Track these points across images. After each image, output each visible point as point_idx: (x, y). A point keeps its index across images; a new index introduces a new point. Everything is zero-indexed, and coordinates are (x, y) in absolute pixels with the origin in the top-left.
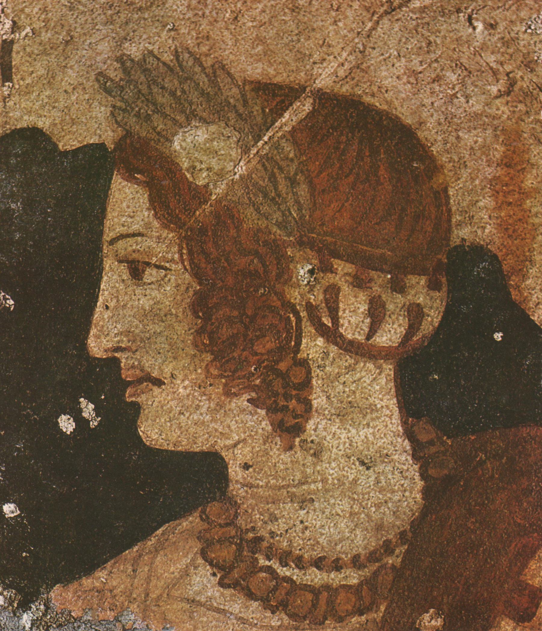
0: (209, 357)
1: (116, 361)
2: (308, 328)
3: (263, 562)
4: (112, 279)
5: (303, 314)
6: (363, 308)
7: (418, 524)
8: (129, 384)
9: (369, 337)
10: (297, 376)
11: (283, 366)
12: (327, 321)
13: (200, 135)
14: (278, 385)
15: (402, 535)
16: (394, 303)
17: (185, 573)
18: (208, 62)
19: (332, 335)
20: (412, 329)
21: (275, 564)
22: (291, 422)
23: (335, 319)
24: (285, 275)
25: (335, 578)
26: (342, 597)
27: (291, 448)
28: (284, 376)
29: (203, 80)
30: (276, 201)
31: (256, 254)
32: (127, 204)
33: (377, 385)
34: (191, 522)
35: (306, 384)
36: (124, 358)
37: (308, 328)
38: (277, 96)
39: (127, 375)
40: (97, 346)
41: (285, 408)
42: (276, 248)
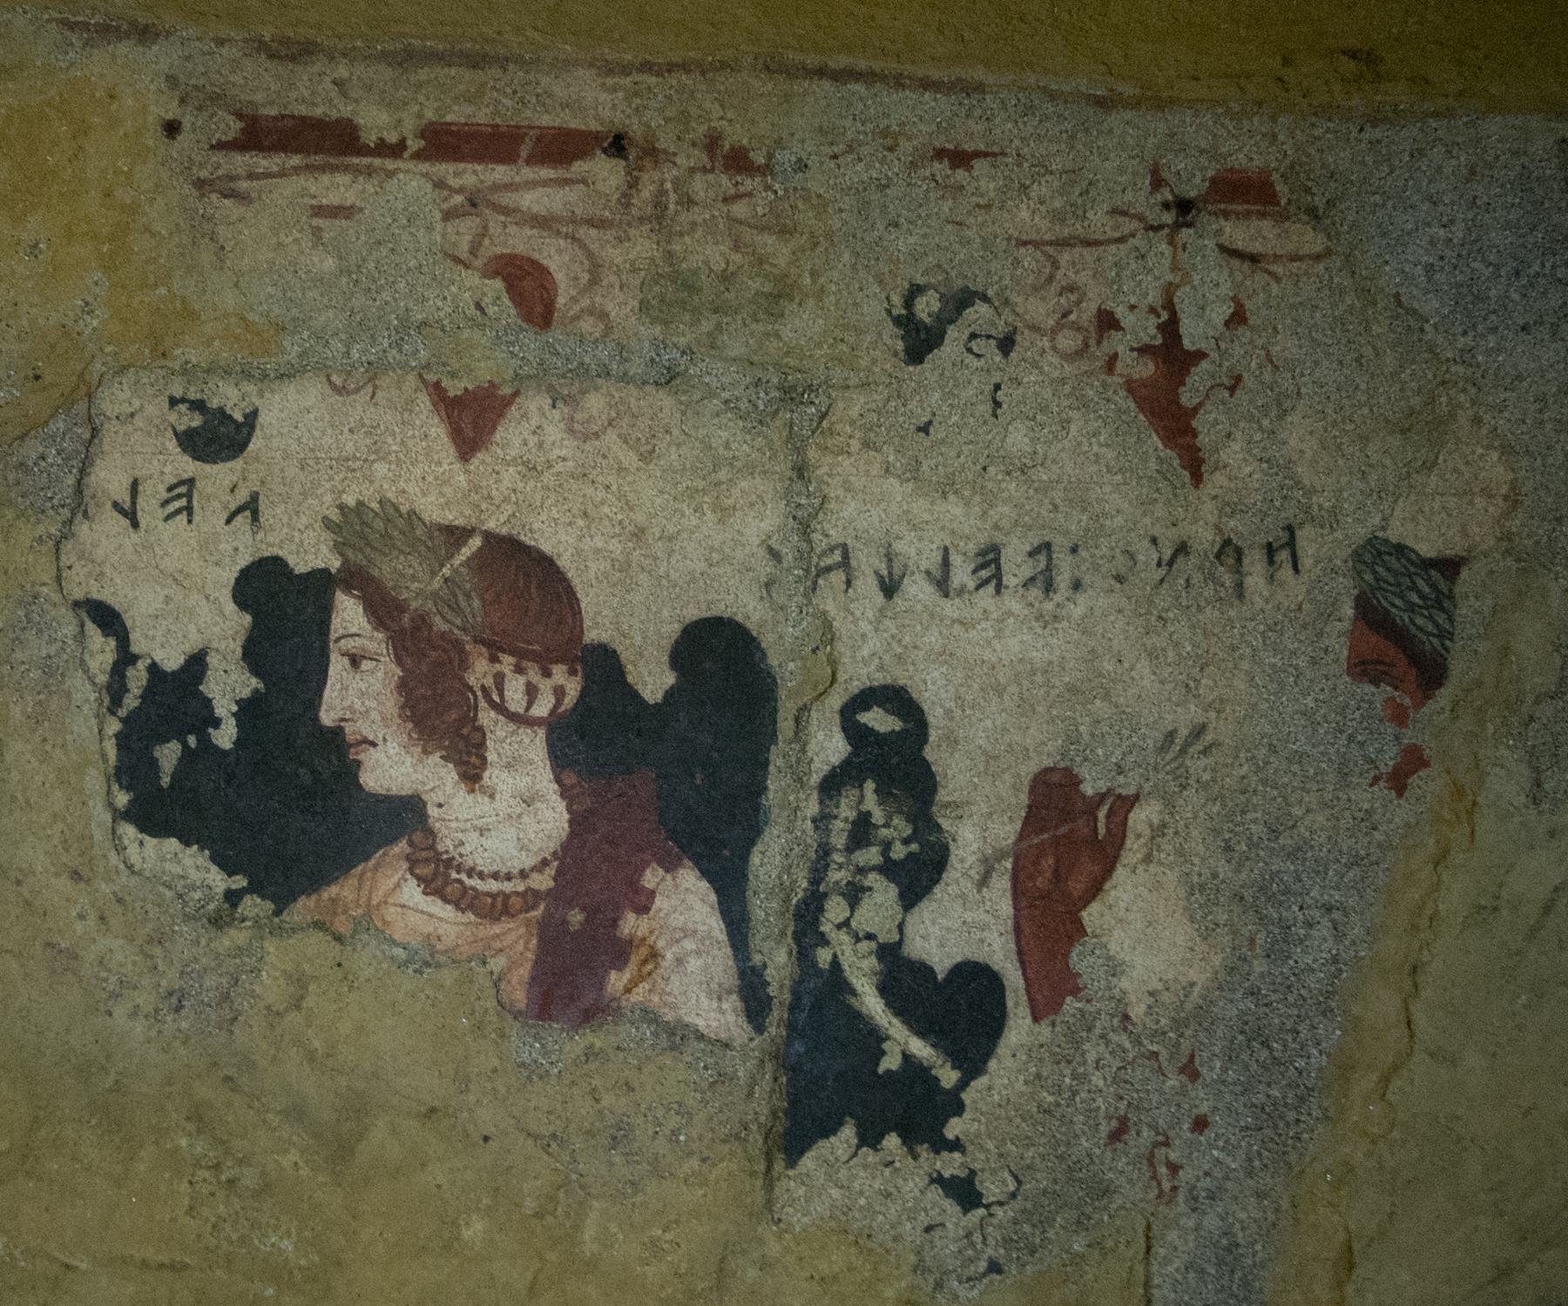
0: (410, 725)
1: (341, 729)
2: (483, 704)
3: (454, 875)
4: (337, 666)
5: (479, 693)
6: (522, 688)
7: (567, 846)
8: (351, 746)
9: (527, 709)
10: (476, 737)
11: (465, 731)
12: (496, 698)
13: (400, 563)
14: (461, 745)
15: (555, 853)
16: (545, 686)
17: (398, 885)
18: (404, 509)
19: (500, 708)
20: (559, 702)
21: (463, 877)
22: (473, 772)
23: (501, 695)
24: (464, 665)
25: (508, 887)
26: (513, 900)
27: (473, 791)
28: (466, 739)
29: (400, 522)
30: (457, 610)
31: (444, 650)
32: (349, 613)
33: (534, 746)
34: (402, 846)
35: (482, 745)
36: (348, 728)
37: (483, 704)
38: (456, 535)
39: (350, 738)
40: (327, 718)
41: (468, 763)
42: (458, 645)
